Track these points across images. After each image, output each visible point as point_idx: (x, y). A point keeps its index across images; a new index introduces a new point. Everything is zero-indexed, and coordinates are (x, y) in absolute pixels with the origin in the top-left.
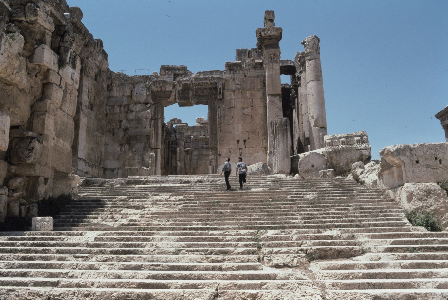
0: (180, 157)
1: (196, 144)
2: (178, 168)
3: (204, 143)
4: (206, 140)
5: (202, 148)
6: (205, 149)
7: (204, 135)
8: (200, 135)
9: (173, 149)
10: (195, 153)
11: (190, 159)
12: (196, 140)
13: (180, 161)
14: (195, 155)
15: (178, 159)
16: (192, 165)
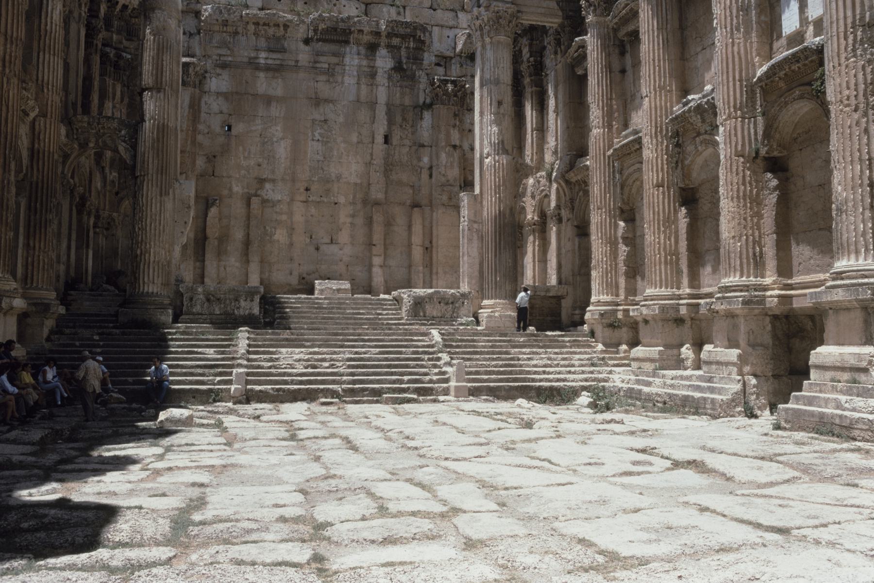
0: (159, 70)
1: (224, 44)
2: (147, 125)
3: (262, 43)
4: (271, 31)
5: (253, 64)
6: (268, 69)
7: (262, 9)
8: (247, 7)
9: (112, 53)
10: (218, 83)
11: (195, 107)
12: (225, 23)
13: (158, 88)
14: (218, 94)
15: (147, 79)
16: (200, 138)
